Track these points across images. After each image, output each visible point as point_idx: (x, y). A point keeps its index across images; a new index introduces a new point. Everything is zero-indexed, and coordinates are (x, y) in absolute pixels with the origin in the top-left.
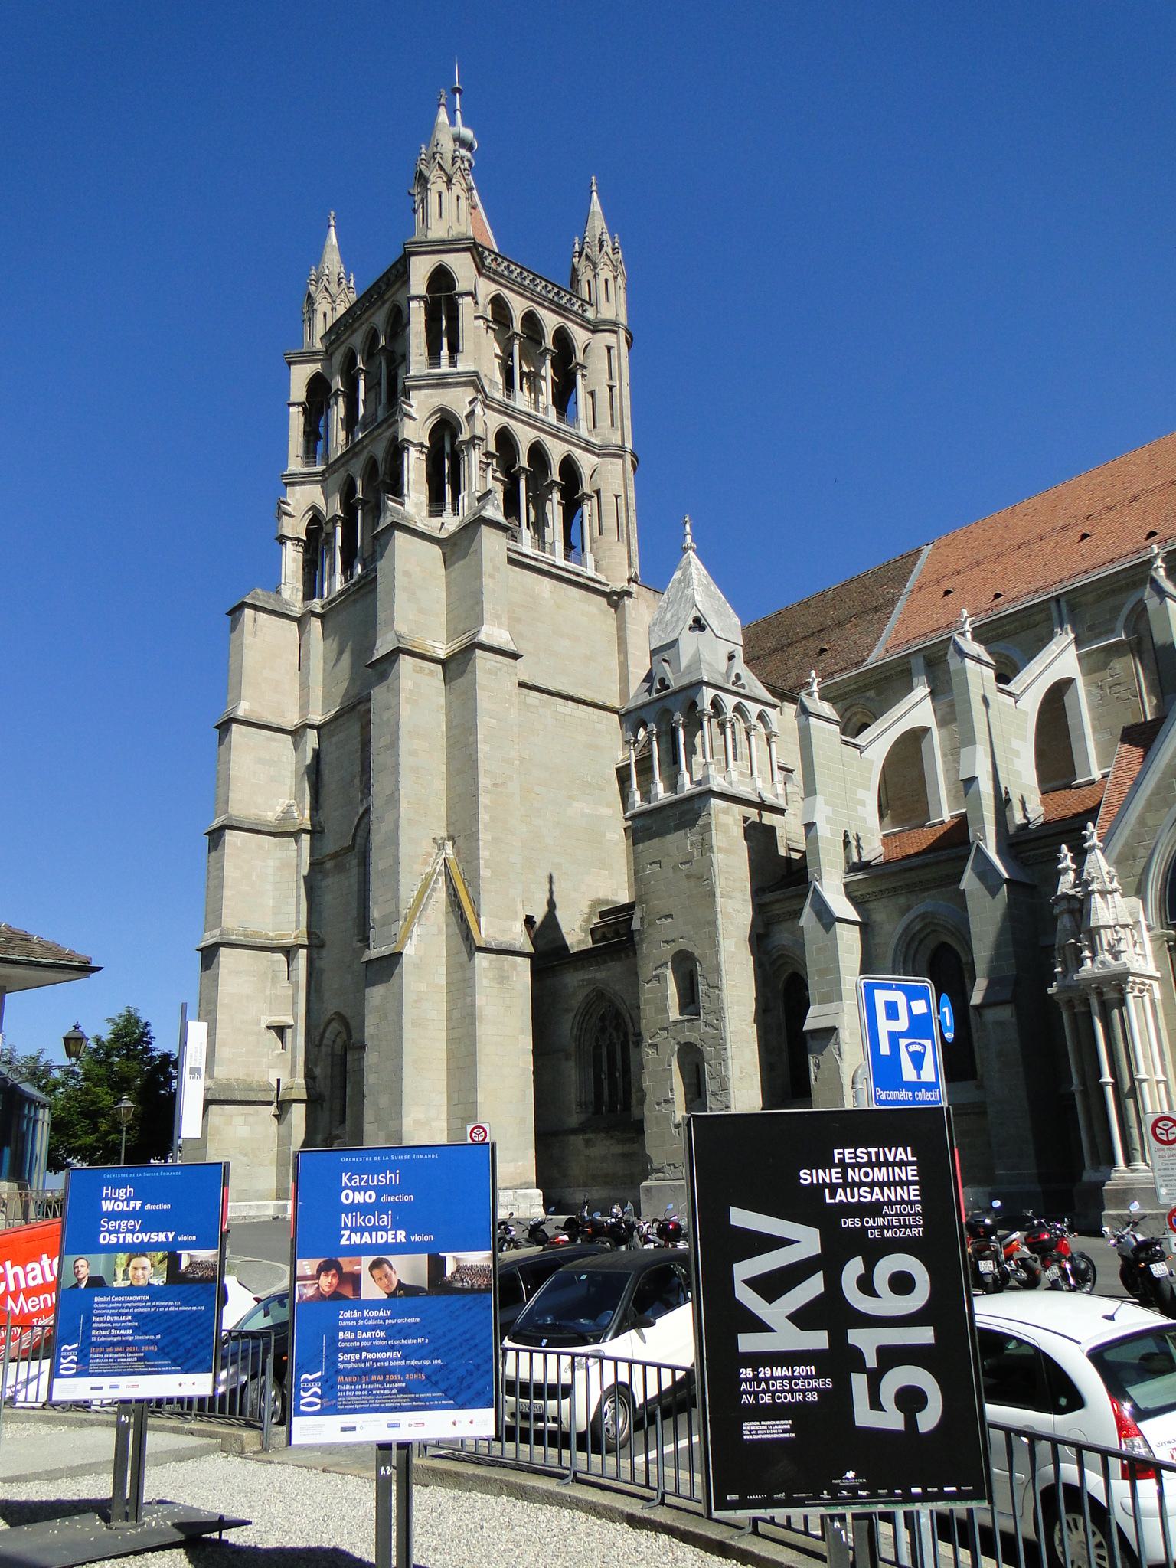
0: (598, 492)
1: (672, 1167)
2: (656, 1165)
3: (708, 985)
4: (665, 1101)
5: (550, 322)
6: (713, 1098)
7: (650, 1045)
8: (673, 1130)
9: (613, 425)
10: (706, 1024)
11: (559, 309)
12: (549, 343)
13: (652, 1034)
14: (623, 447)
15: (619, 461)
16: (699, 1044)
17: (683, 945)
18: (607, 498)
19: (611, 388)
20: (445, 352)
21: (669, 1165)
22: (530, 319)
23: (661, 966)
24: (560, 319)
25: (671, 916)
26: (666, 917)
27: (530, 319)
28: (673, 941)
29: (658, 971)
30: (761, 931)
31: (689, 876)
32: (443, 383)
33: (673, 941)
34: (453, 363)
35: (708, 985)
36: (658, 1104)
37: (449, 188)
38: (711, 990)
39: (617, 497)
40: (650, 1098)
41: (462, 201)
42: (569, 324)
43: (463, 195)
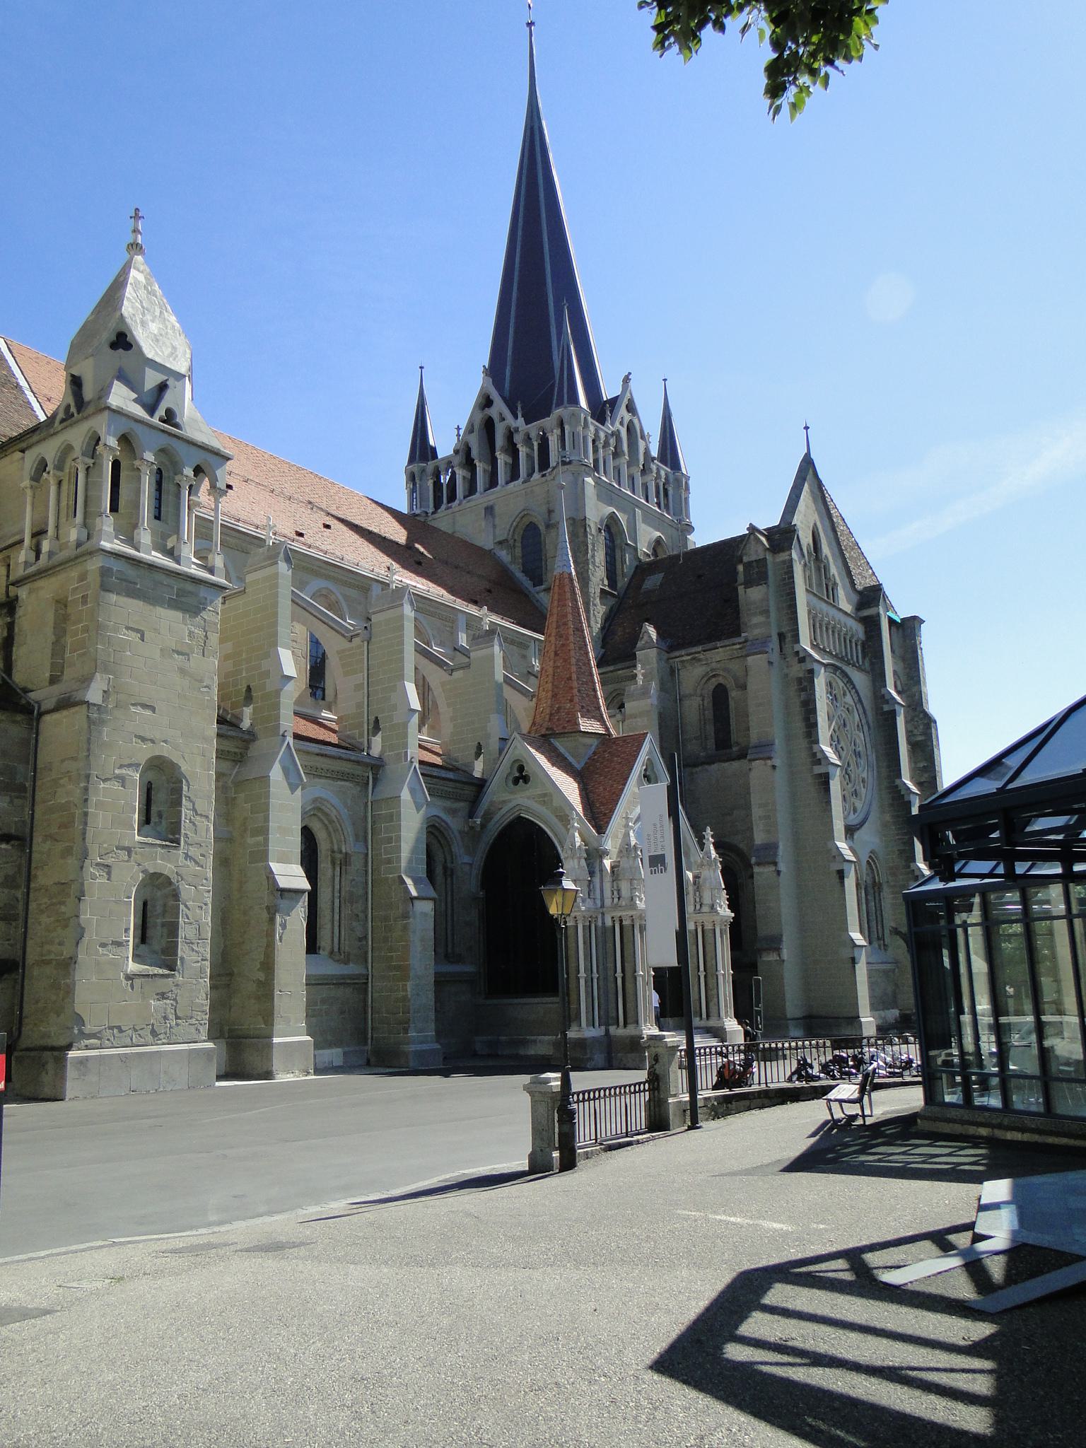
1: (115, 1031)
2: (88, 1028)
3: (194, 810)
4: (114, 943)
6: (186, 947)
7: (98, 864)
8: (124, 982)
10: (187, 856)
13: (103, 852)
16: (174, 879)
17: (165, 750)
21: (111, 1028)
23: (129, 766)
25: (153, 709)
26: (145, 706)
28: (153, 741)
29: (123, 771)
31: (182, 671)
33: (153, 741)
35: (194, 810)
36: (103, 945)
38: (198, 818)
40: (91, 936)
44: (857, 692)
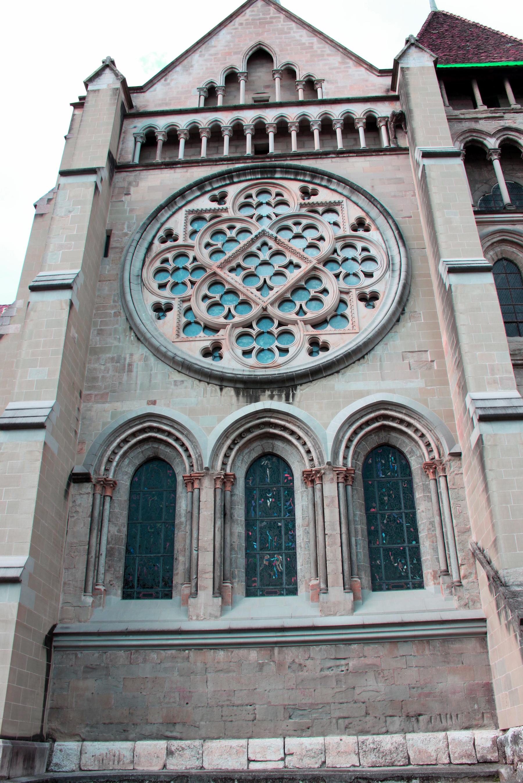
44: (341, 181)
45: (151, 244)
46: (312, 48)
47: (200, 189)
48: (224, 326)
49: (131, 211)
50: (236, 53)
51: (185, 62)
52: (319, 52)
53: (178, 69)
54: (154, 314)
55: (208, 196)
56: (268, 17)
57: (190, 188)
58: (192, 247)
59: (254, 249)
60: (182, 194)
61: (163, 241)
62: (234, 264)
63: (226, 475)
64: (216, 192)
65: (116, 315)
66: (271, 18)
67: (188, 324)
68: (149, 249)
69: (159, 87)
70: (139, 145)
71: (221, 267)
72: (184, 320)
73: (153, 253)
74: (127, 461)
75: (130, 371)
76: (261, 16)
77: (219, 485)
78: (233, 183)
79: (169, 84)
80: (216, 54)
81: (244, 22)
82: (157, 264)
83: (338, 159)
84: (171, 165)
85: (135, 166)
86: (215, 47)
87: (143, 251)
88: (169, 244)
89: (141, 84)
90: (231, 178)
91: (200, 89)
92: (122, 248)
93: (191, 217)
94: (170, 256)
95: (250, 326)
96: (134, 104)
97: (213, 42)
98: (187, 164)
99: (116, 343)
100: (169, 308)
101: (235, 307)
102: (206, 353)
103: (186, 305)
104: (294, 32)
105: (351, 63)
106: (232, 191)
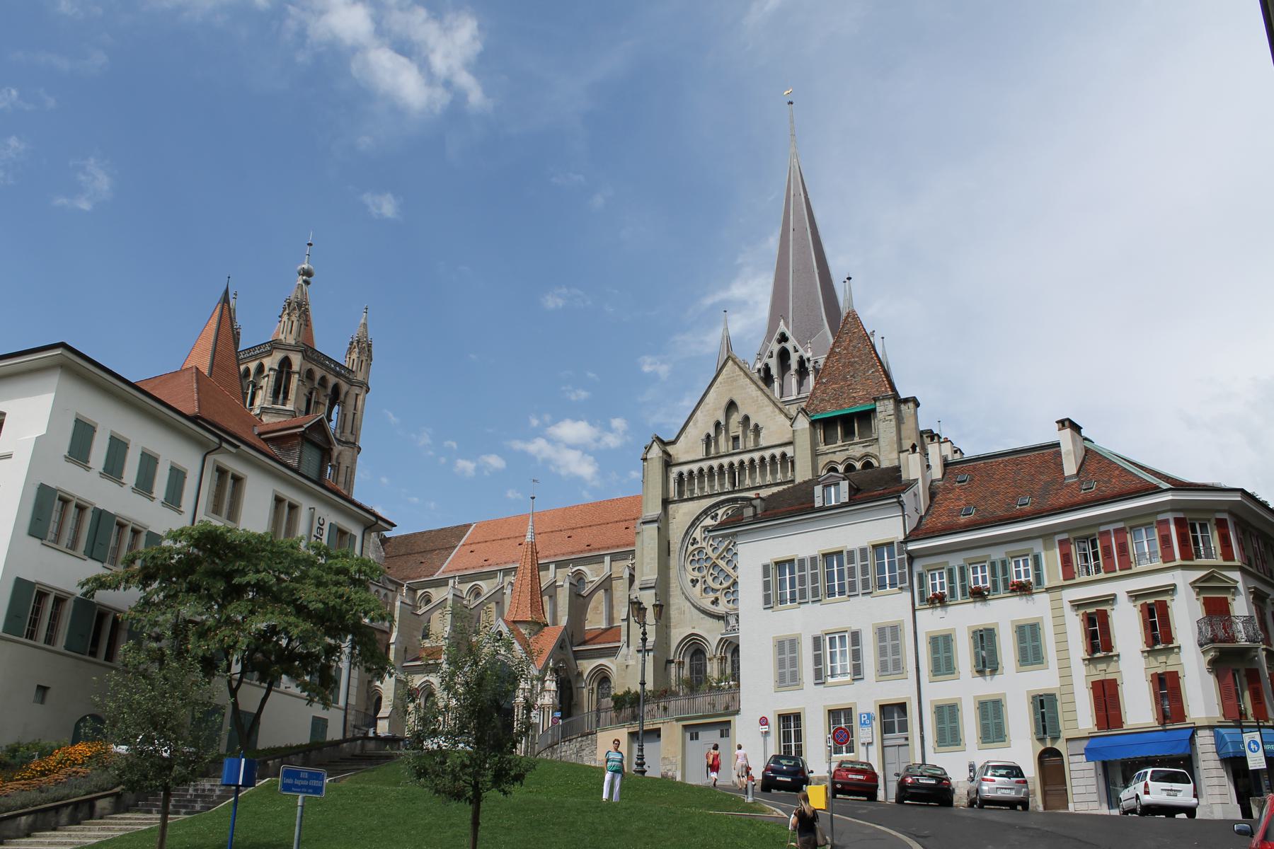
0: (339, 463)
5: (332, 380)
9: (352, 432)
11: (338, 375)
12: (329, 391)
14: (354, 444)
15: (351, 450)
18: (343, 468)
19: (354, 414)
20: (281, 396)
22: (323, 379)
24: (337, 379)
27: (323, 379)
30: (370, 679)
32: (278, 412)
34: (284, 404)
37: (298, 320)
39: (347, 467)
41: (303, 326)
42: (341, 381)
43: (303, 323)
45: (687, 547)
46: (757, 400)
47: (705, 514)
48: (718, 590)
49: (677, 528)
50: (719, 409)
51: (694, 419)
52: (761, 405)
53: (691, 424)
54: (691, 584)
55: (709, 517)
56: (734, 375)
57: (700, 514)
58: (704, 548)
59: (730, 547)
60: (697, 518)
61: (692, 544)
62: (722, 556)
63: (722, 657)
64: (713, 514)
65: (676, 586)
66: (737, 376)
67: (705, 588)
68: (686, 551)
69: (682, 438)
70: (676, 484)
71: (717, 559)
72: (704, 587)
73: (688, 553)
74: (687, 652)
75: (684, 613)
76: (732, 375)
77: (719, 661)
78: (720, 508)
79: (687, 436)
80: (708, 410)
81: (722, 381)
82: (691, 558)
83: (767, 489)
84: (692, 499)
85: (676, 501)
86: (708, 404)
87: (684, 552)
88: (695, 546)
89: (673, 439)
90: (719, 506)
91: (703, 440)
92: (675, 551)
93: (703, 529)
94: (696, 553)
95: (729, 588)
96: (671, 453)
97: (707, 400)
98: (699, 498)
99: (677, 601)
100: (697, 581)
101: (724, 579)
102: (713, 603)
103: (703, 580)
104: (750, 388)
105: (777, 411)
106: (720, 512)
